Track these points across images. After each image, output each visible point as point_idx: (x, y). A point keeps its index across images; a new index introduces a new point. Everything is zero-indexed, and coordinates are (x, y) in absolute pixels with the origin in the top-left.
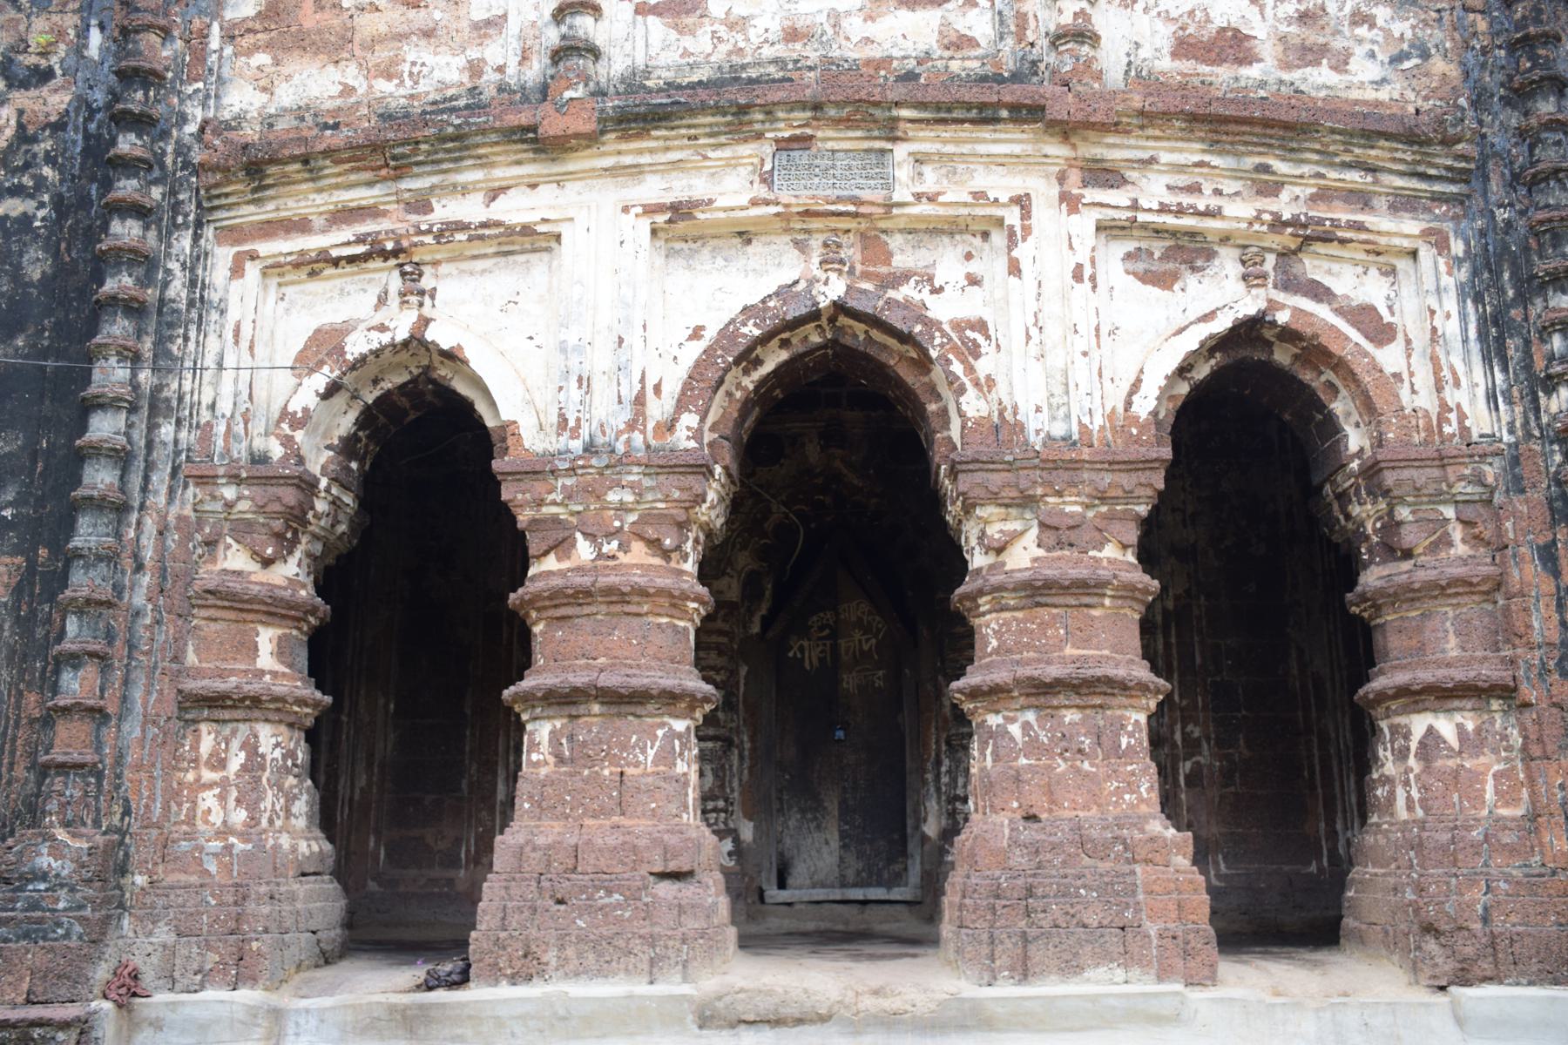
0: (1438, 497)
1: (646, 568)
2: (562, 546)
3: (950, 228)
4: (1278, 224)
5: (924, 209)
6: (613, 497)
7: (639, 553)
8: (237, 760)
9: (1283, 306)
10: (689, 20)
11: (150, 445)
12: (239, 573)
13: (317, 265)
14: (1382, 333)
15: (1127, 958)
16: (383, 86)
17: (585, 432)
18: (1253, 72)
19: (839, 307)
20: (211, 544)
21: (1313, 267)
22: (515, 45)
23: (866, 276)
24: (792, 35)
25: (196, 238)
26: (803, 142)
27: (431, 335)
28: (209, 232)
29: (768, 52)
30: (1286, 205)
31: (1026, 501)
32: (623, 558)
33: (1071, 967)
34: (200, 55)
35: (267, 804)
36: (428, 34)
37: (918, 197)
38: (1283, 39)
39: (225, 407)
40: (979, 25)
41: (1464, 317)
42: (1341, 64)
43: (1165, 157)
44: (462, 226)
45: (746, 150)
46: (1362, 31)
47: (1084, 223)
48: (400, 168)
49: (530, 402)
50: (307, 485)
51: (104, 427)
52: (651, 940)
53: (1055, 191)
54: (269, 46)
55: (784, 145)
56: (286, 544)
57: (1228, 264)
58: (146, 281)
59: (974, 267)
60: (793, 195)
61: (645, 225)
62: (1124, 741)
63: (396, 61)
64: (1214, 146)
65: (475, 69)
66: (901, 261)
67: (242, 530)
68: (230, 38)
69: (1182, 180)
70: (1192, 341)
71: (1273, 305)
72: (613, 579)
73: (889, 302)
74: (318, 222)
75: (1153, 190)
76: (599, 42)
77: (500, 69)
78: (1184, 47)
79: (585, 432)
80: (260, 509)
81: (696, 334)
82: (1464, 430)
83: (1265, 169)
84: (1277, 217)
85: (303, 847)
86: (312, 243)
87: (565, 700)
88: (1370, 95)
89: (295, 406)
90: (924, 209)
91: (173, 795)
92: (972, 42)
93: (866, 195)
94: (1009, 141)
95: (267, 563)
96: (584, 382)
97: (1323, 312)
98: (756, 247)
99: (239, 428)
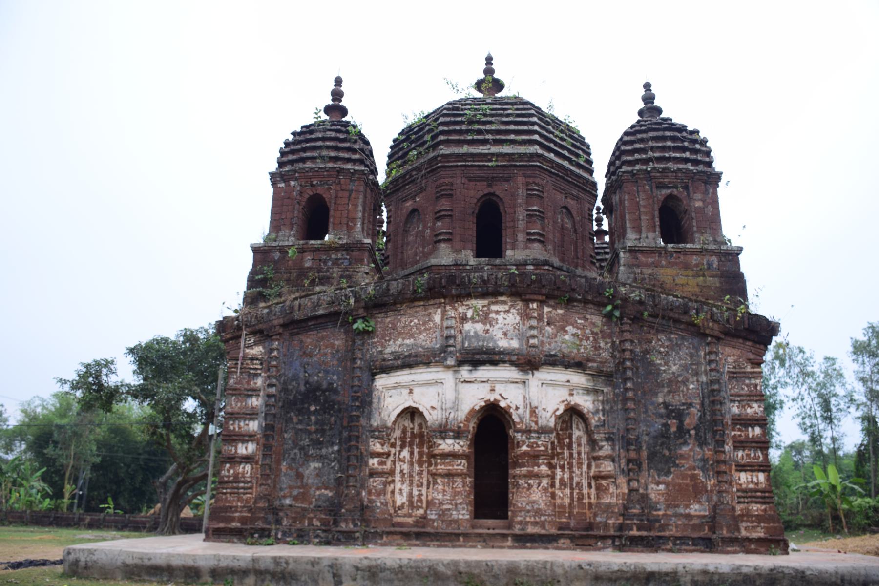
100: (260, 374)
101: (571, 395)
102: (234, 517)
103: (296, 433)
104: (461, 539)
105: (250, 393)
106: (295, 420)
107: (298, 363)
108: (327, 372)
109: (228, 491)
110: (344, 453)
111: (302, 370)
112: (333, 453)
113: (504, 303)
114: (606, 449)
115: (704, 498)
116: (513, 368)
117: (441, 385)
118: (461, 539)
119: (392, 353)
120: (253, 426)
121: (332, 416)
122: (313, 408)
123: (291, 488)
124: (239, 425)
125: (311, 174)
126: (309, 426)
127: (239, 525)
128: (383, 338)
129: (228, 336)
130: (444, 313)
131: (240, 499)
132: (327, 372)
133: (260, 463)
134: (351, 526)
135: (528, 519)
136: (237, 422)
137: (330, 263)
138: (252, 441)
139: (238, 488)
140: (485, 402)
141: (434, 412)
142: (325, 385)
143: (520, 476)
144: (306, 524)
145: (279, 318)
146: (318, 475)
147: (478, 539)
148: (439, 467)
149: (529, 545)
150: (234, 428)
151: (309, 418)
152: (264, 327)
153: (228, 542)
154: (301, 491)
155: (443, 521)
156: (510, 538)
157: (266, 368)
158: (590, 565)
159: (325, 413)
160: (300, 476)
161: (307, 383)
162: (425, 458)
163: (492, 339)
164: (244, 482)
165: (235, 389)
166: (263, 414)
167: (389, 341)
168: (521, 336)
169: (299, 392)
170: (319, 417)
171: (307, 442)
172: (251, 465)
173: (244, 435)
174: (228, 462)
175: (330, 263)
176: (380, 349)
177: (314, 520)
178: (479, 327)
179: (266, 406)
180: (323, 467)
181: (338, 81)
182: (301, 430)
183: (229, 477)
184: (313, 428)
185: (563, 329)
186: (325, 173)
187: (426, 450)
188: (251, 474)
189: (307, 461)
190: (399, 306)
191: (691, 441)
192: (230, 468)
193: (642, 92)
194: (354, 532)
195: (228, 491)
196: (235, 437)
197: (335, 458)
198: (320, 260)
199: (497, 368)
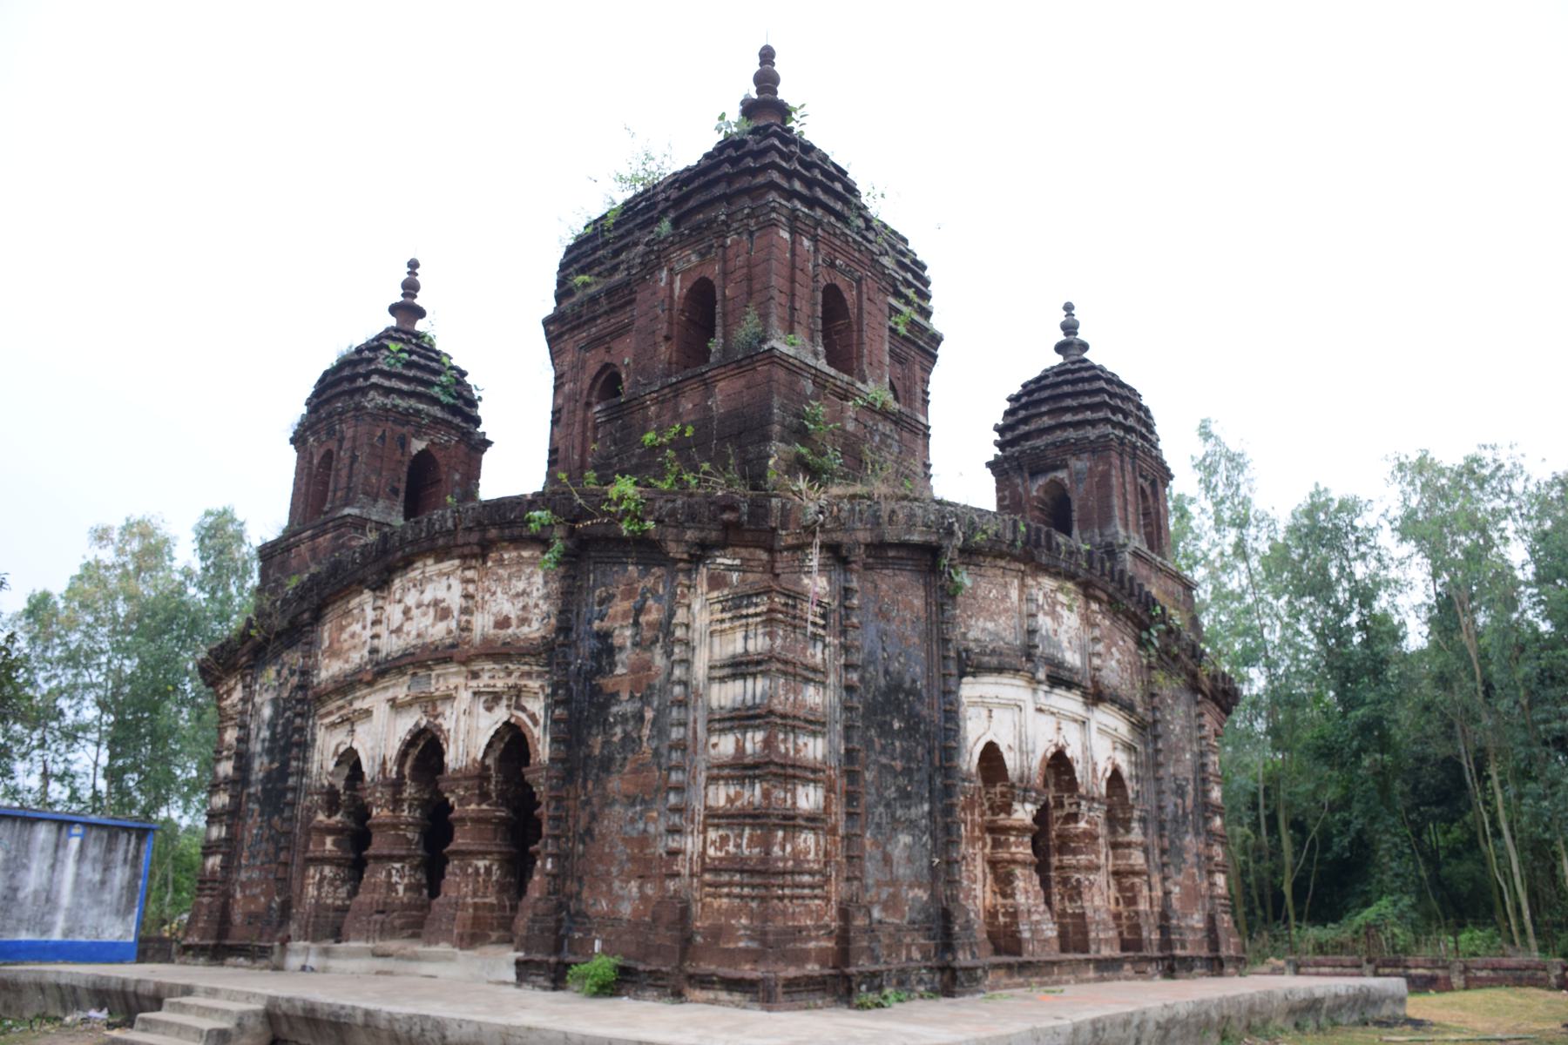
8: (318, 877)
12: (321, 822)
13: (333, 725)
18: (510, 631)
20: (316, 812)
24: (419, 635)
26: (414, 674)
30: (511, 681)
31: (452, 792)
36: (355, 647)
41: (546, 716)
51: (291, 781)
52: (368, 931)
57: (504, 702)
58: (301, 736)
60: (415, 692)
64: (495, 662)
75: (485, 679)
94: (453, 668)
95: (329, 817)
100: (823, 637)
101: (1115, 749)
102: (808, 952)
103: (880, 772)
104: (1056, 969)
105: (811, 675)
106: (877, 747)
107: (872, 631)
108: (908, 657)
109: (787, 891)
110: (939, 819)
111: (880, 645)
112: (923, 817)
113: (1067, 594)
114: (1136, 835)
115: (1200, 907)
116: (1081, 699)
117: (1017, 709)
118: (1056, 969)
119: (976, 640)
120: (814, 749)
121: (918, 744)
122: (896, 725)
123: (879, 884)
124: (795, 743)
125: (838, 243)
126: (894, 759)
127: (817, 967)
128: (964, 611)
129: (790, 541)
130: (1023, 586)
131: (810, 912)
132: (908, 657)
133: (841, 831)
134: (969, 957)
135: (1102, 936)
136: (791, 736)
137: (877, 438)
138: (815, 781)
139: (803, 886)
140: (1056, 745)
141: (1012, 754)
142: (907, 685)
143: (1077, 869)
144: (904, 959)
145: (865, 529)
146: (910, 860)
147: (1068, 969)
148: (1013, 849)
149: (1105, 974)
150: (787, 749)
151: (893, 743)
152: (845, 540)
153: (807, 1008)
154: (891, 890)
155: (1039, 941)
156: (1091, 966)
157: (838, 629)
158: (1291, 993)
159: (910, 736)
160: (887, 860)
161: (887, 672)
162: (977, 833)
163: (1058, 646)
164: (812, 873)
165: (786, 662)
166: (839, 727)
167: (970, 617)
168: (1082, 649)
169: (878, 688)
170: (905, 744)
171: (891, 793)
172: (815, 834)
173: (805, 768)
174: (784, 828)
175: (877, 438)
176: (963, 630)
177: (913, 948)
178: (1048, 620)
179: (848, 709)
180: (914, 843)
181: (767, 55)
182: (884, 766)
183: (785, 859)
184: (898, 765)
185: (1109, 649)
186: (857, 254)
187: (978, 819)
188: (817, 854)
189: (894, 830)
190: (981, 559)
191: (1190, 829)
192: (784, 839)
193: (1061, 316)
194: (975, 969)
195: (787, 891)
196: (790, 771)
197: (926, 826)
198: (866, 427)
199: (1069, 695)
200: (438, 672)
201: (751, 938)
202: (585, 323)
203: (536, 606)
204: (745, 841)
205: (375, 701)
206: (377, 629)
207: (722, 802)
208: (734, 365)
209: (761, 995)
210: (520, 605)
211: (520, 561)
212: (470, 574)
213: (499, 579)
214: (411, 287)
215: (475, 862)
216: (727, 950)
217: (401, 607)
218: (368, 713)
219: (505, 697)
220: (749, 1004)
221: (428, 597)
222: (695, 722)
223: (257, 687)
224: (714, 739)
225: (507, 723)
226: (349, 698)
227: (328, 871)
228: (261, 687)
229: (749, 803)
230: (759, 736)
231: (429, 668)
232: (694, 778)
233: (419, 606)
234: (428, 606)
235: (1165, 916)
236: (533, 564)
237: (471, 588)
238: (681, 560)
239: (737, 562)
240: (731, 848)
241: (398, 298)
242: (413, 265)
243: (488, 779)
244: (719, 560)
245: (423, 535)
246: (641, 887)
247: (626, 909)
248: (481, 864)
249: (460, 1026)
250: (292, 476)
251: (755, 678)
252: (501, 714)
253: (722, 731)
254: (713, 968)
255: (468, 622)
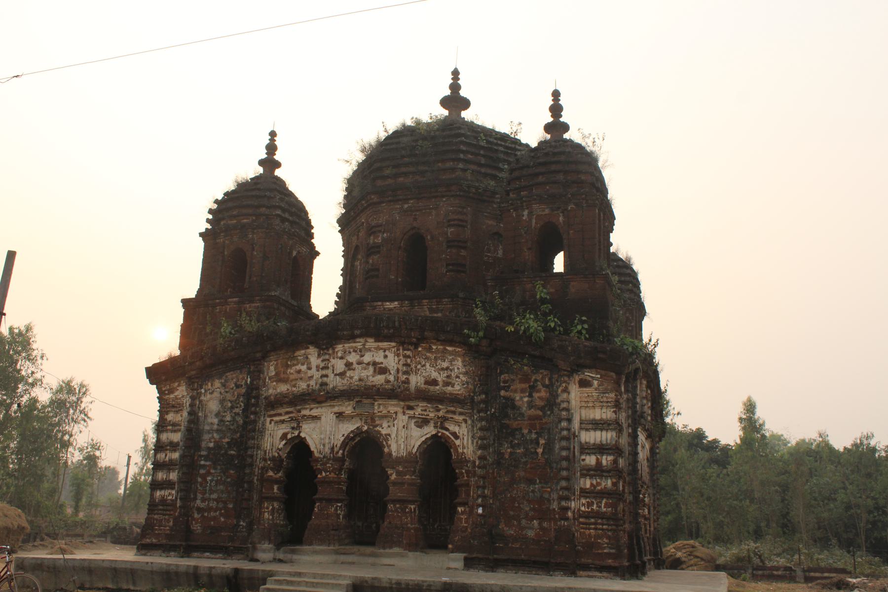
0: (462, 469)
1: (333, 477)
2: (321, 474)
3: (385, 417)
4: (438, 418)
5: (380, 414)
6: (328, 465)
7: (333, 475)
9: (440, 432)
10: (343, 377)
11: (257, 455)
12: (271, 476)
13: (283, 422)
14: (457, 437)
15: (399, 546)
16: (294, 389)
17: (323, 454)
18: (438, 387)
19: (366, 431)
20: (267, 471)
21: (447, 425)
22: (315, 381)
23: (371, 425)
24: (360, 380)
25: (264, 417)
26: (360, 401)
27: (301, 434)
28: (266, 416)
29: (356, 383)
30: (441, 414)
31: (393, 468)
32: (330, 476)
33: (391, 547)
34: (265, 383)
35: (275, 515)
36: (301, 379)
37: (379, 412)
38: (444, 381)
39: (268, 448)
40: (391, 378)
42: (453, 386)
43: (420, 405)
44: (305, 416)
45: (351, 402)
46: (457, 379)
47: (406, 418)
48: (296, 405)
49: (316, 448)
50: (282, 461)
53: (402, 411)
54: (276, 381)
55: (357, 402)
56: (278, 471)
57: (432, 424)
59: (389, 424)
60: (358, 411)
61: (335, 416)
62: (407, 510)
63: (296, 384)
65: (308, 386)
66: (377, 422)
67: (272, 469)
68: (270, 379)
69: (424, 408)
70: (423, 439)
71: (438, 432)
72: (327, 480)
73: (375, 431)
74: (283, 414)
75: (418, 411)
76: (328, 382)
77: (312, 386)
78: (426, 383)
79: (323, 454)
80: (274, 465)
81: (343, 435)
82: (465, 457)
83: (437, 407)
84: (438, 416)
85: (282, 523)
86: (282, 418)
87: (320, 500)
88: (457, 392)
89: (280, 447)
90: (380, 414)
91: (260, 514)
92: (390, 381)
93: (370, 411)
94: (394, 402)
95: (276, 474)
96: (324, 445)
97: (447, 433)
98: (354, 420)
99: (271, 451)
181: (556, 94)
200: (380, 402)
201: (611, 548)
202: (400, 200)
203: (457, 377)
204: (603, 505)
205: (327, 414)
206: (324, 372)
207: (588, 486)
208: (582, 276)
209: (620, 573)
210: (445, 375)
211: (445, 351)
212: (408, 353)
213: (427, 358)
214: (271, 148)
215: (410, 506)
216: (599, 554)
217: (345, 361)
218: (316, 418)
219: (432, 422)
220: (613, 578)
221: (367, 358)
222: (574, 448)
223: (203, 391)
224: (583, 457)
225: (434, 436)
226: (298, 408)
227: (276, 505)
228: (206, 391)
229: (605, 487)
230: (610, 458)
231: (375, 400)
232: (575, 474)
233: (359, 363)
234: (368, 364)
235: (654, 540)
236: (453, 355)
237: (409, 361)
238: (565, 370)
239: (599, 376)
240: (595, 507)
241: (264, 156)
242: (273, 134)
243: (417, 462)
244: (586, 374)
245: (372, 325)
246: (540, 524)
247: (531, 534)
248: (412, 507)
249: (521, 589)
250: (201, 257)
251: (607, 431)
252: (430, 430)
253: (589, 454)
254: (590, 561)
255: (407, 379)
